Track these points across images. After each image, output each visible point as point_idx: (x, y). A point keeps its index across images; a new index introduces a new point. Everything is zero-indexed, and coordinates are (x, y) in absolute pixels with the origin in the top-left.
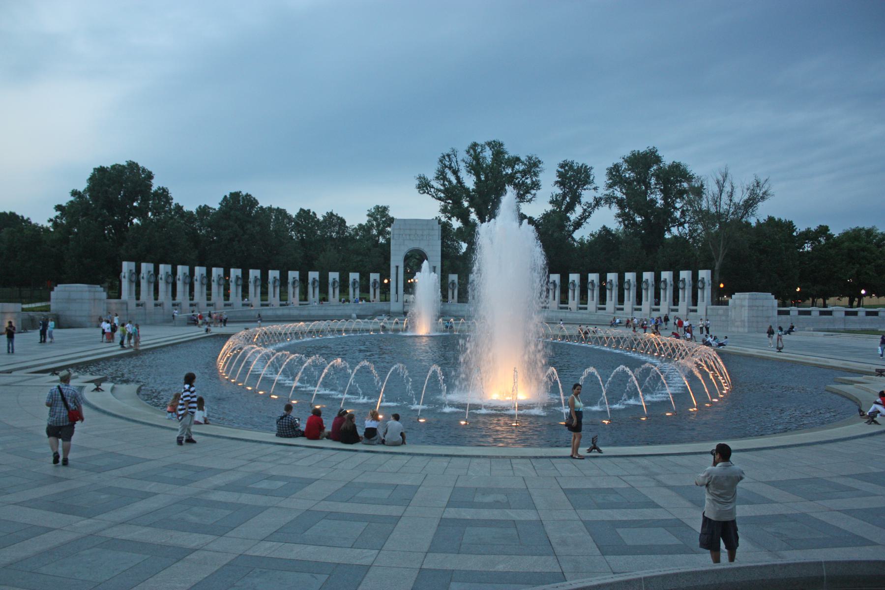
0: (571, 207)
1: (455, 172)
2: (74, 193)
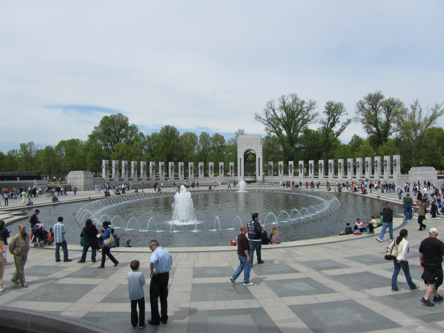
0: (333, 125)
1: (274, 111)
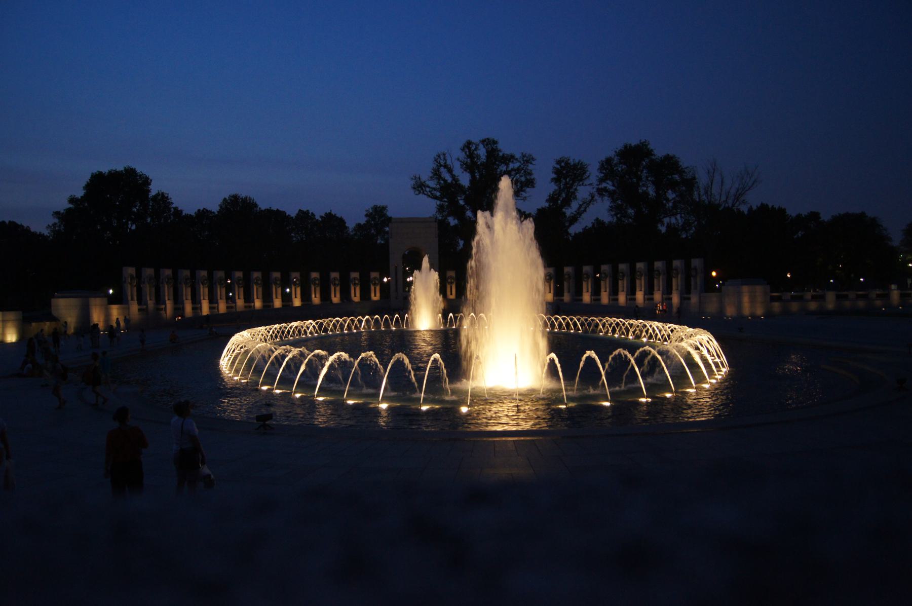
1: (450, 171)
2: (72, 200)
